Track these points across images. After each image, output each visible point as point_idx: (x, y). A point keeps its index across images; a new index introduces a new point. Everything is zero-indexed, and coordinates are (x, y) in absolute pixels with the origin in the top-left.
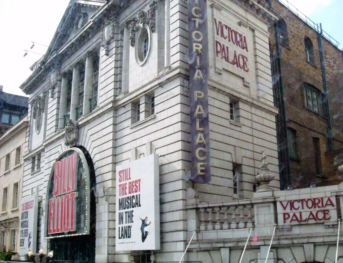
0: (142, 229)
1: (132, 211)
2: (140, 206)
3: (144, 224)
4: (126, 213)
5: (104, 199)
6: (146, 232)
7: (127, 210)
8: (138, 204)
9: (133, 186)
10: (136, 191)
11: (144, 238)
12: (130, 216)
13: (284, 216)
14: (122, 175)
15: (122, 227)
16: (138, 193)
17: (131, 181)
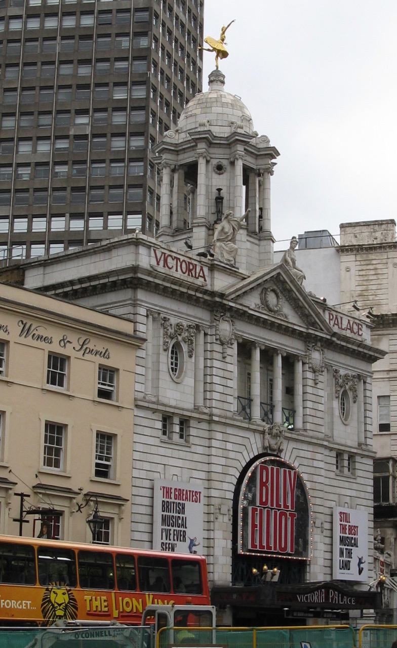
0: (359, 565)
1: (351, 549)
2: (357, 547)
3: (360, 562)
4: (346, 549)
5: (319, 530)
6: (362, 568)
7: (346, 547)
8: (356, 545)
9: (352, 530)
10: (355, 535)
11: (360, 572)
12: (350, 553)
14: (342, 516)
15: (343, 561)
16: (356, 536)
17: (350, 524)
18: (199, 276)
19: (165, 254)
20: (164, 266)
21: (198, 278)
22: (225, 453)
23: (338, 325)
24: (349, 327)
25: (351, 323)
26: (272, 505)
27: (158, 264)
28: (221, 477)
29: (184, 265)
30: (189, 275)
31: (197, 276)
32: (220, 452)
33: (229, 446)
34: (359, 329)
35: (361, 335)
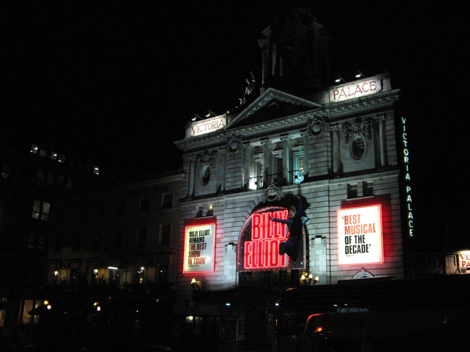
13: (463, 263)
18: (220, 125)
19: (198, 126)
20: (198, 132)
21: (219, 127)
22: (234, 215)
23: (345, 94)
24: (358, 90)
25: (361, 87)
26: (264, 237)
27: (194, 133)
28: (230, 230)
29: (210, 125)
30: (213, 128)
31: (218, 126)
32: (231, 215)
33: (237, 210)
34: (371, 86)
35: (375, 89)
